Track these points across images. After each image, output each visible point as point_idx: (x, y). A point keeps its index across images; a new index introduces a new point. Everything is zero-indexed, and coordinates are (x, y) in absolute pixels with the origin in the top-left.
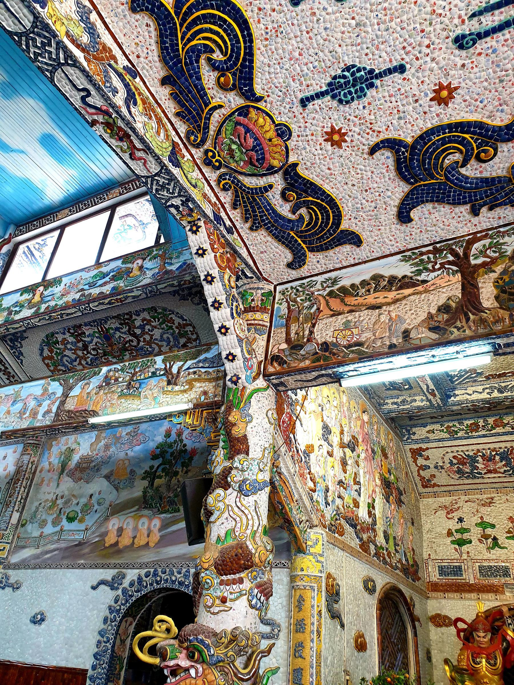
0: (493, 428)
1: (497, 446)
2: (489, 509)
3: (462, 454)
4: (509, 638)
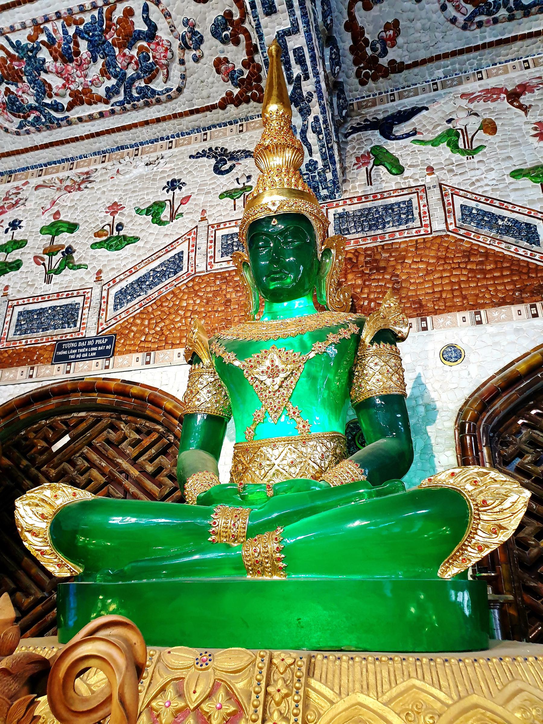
2: (76, 195)
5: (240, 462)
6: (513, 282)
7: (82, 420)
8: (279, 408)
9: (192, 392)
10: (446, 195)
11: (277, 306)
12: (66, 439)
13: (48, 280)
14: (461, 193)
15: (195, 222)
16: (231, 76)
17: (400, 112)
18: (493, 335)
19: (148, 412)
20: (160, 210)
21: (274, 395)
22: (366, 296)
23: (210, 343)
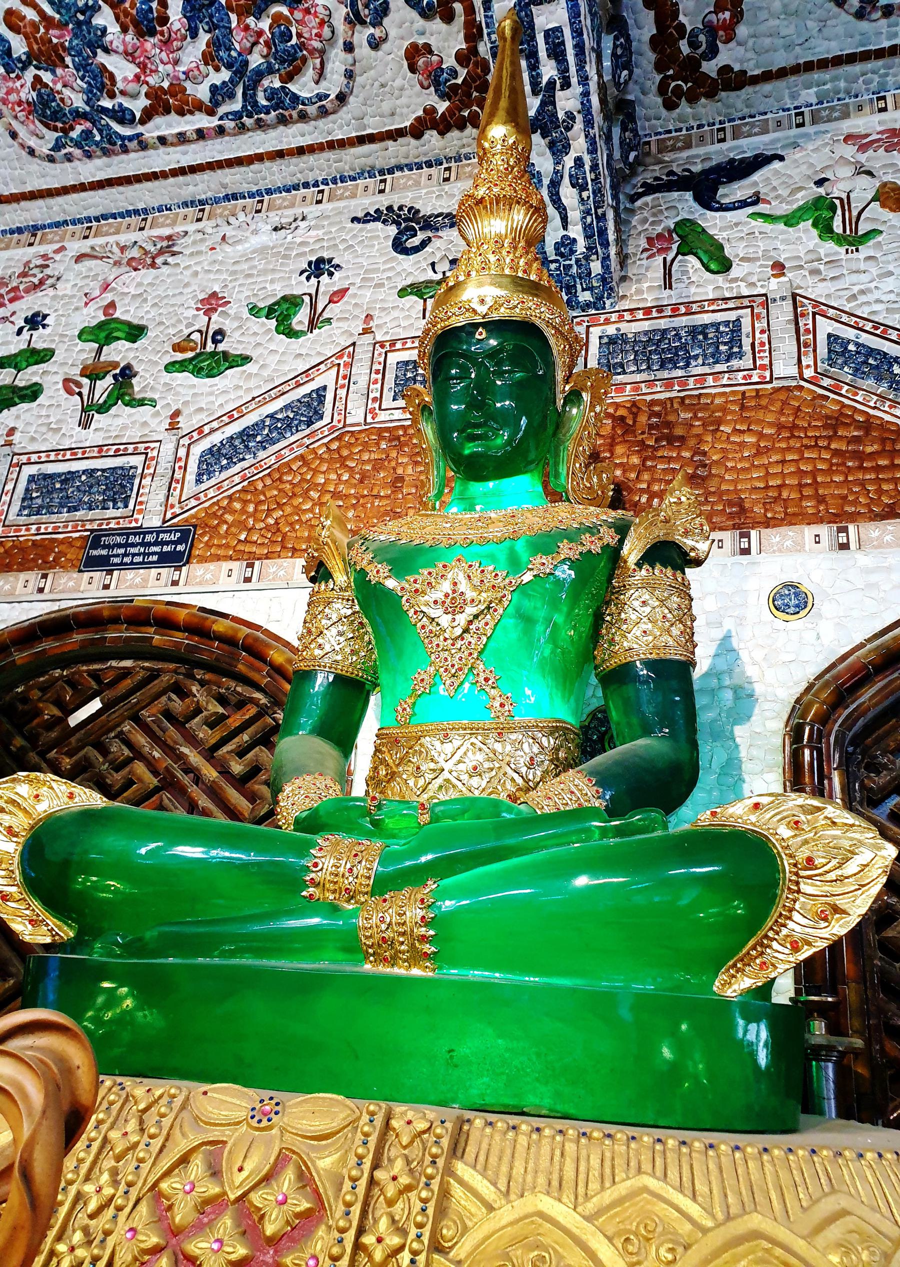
2: (146, 275)
5: (383, 761)
8: (460, 669)
9: (309, 632)
10: (803, 315)
11: (476, 488)
13: (85, 424)
14: (831, 313)
15: (352, 335)
16: (435, 78)
17: (732, 161)
18: (868, 571)
19: (241, 667)
20: (292, 311)
21: (453, 645)
22: (644, 486)
23: (350, 546)
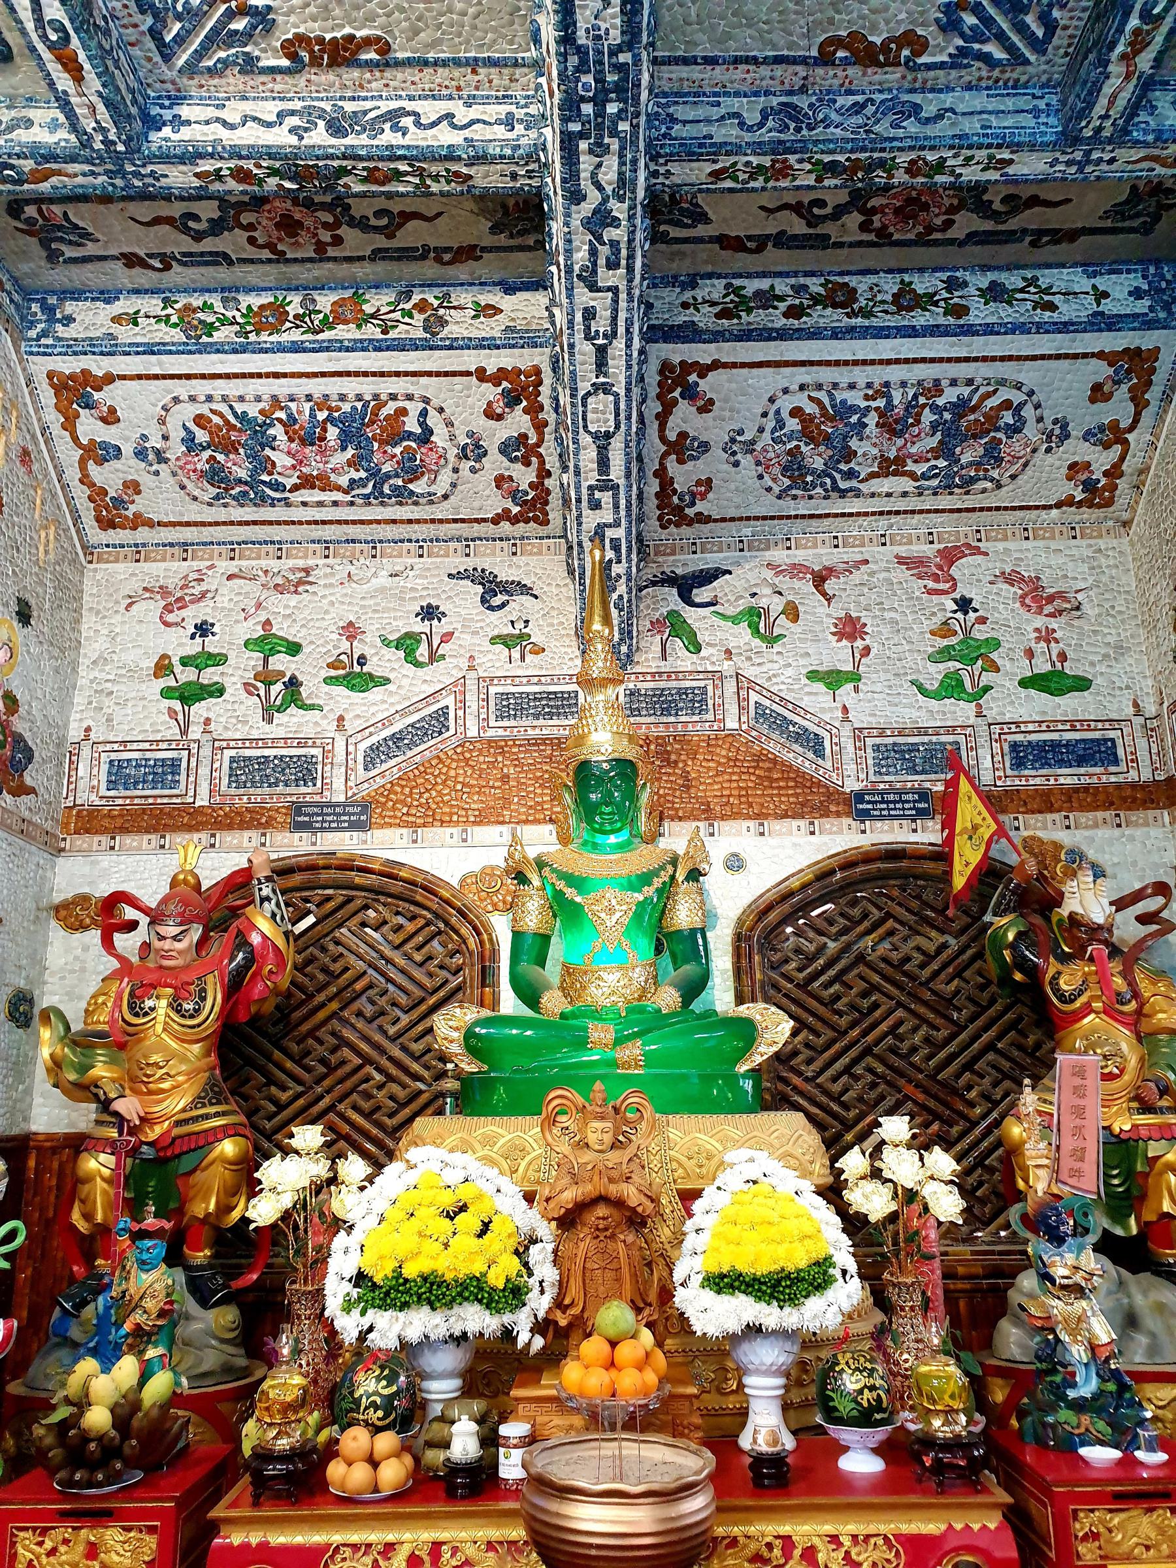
0: (327, 324)
1: (333, 387)
2: (293, 600)
3: (223, 408)
4: (255, 939)
6: (796, 795)
7: (329, 899)
12: (310, 920)
16: (514, 495)
19: (418, 898)
